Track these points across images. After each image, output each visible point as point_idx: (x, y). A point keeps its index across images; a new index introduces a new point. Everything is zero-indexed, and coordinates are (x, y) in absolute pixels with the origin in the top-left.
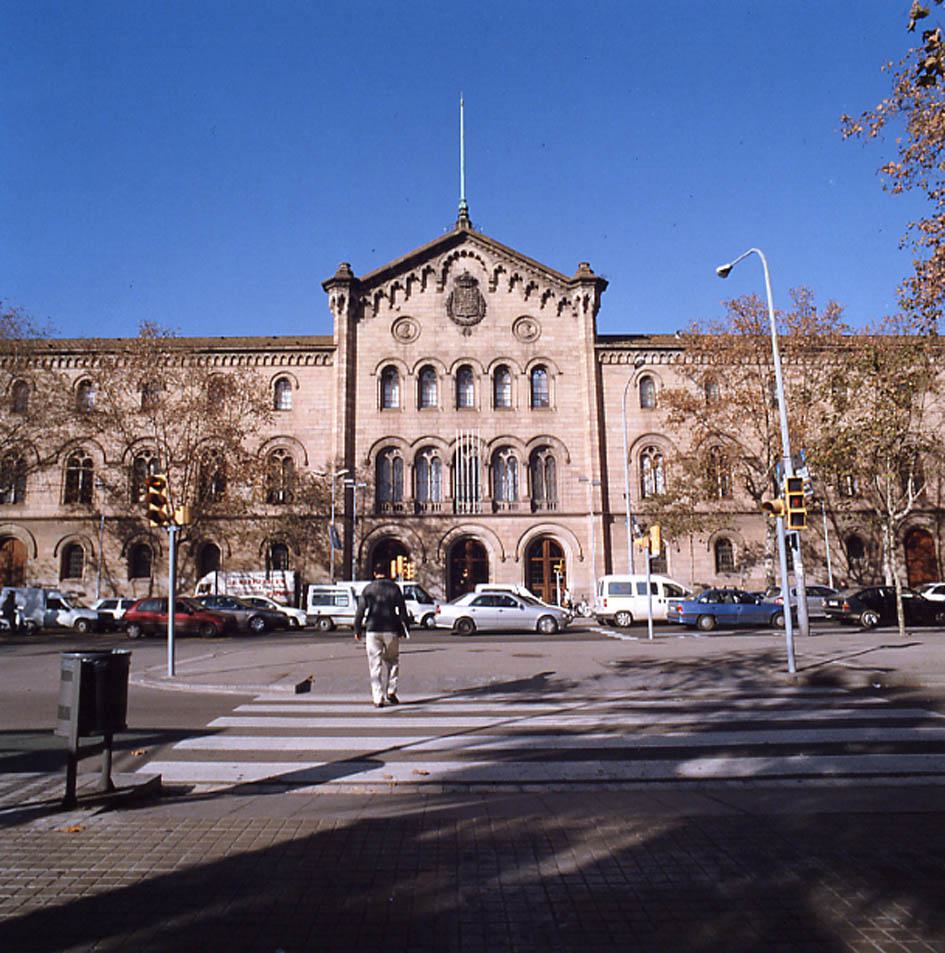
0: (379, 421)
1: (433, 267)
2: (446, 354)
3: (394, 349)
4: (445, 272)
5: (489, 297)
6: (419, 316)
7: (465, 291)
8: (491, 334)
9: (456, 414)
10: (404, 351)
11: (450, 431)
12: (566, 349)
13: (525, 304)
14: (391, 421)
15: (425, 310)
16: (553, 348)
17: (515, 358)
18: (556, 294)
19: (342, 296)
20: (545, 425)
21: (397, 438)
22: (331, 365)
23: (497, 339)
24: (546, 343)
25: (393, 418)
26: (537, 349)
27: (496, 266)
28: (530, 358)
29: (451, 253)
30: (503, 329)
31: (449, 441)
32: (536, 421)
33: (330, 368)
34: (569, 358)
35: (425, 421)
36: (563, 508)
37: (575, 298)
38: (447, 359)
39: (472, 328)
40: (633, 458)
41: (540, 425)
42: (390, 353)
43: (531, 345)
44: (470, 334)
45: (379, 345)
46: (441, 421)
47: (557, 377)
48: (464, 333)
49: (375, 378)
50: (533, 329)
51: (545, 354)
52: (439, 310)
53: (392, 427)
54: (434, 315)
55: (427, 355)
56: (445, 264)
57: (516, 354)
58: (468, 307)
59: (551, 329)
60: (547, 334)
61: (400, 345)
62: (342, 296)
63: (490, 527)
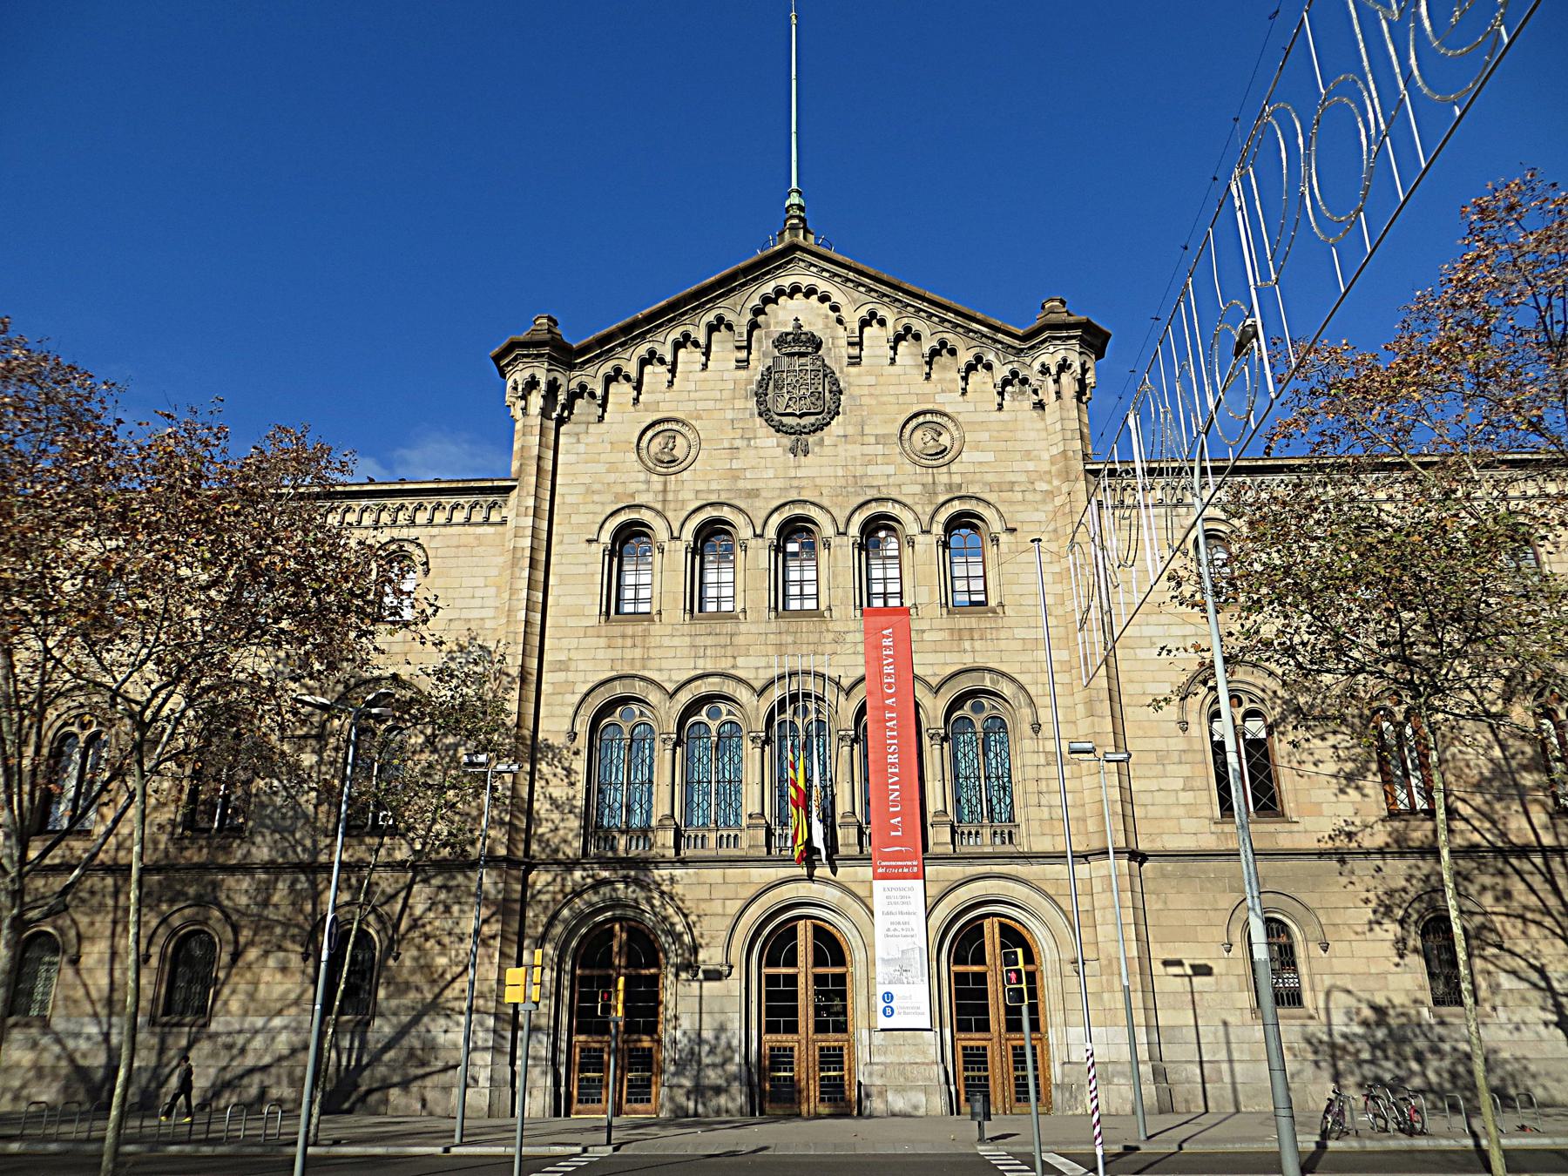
0: (602, 642)
1: (729, 317)
2: (753, 494)
3: (643, 487)
4: (754, 325)
5: (849, 377)
6: (699, 418)
7: (797, 361)
8: (856, 450)
9: (773, 626)
10: (665, 491)
11: (762, 662)
12: (1023, 478)
13: (928, 387)
14: (629, 642)
15: (711, 404)
16: (990, 478)
17: (908, 501)
18: (996, 364)
19: (533, 377)
20: (978, 645)
21: (643, 679)
22: (504, 522)
23: (870, 461)
24: (975, 466)
25: (633, 637)
26: (957, 479)
27: (863, 312)
28: (942, 499)
29: (768, 288)
30: (879, 439)
31: (758, 685)
32: (958, 635)
33: (500, 528)
34: (1029, 496)
35: (710, 641)
36: (1032, 839)
37: (1037, 366)
38: (758, 503)
39: (811, 439)
40: (1192, 718)
41: (967, 645)
42: (632, 496)
43: (944, 469)
44: (806, 453)
45: (612, 478)
46: (740, 640)
47: (1004, 538)
48: (793, 451)
49: (597, 549)
50: (945, 440)
51: (973, 490)
52: (739, 404)
53: (629, 654)
54: (730, 415)
55: (714, 498)
56: (758, 311)
57: (910, 492)
58: (802, 396)
59: (985, 436)
60: (977, 447)
61: (655, 478)
62: (533, 377)
63: (853, 887)
